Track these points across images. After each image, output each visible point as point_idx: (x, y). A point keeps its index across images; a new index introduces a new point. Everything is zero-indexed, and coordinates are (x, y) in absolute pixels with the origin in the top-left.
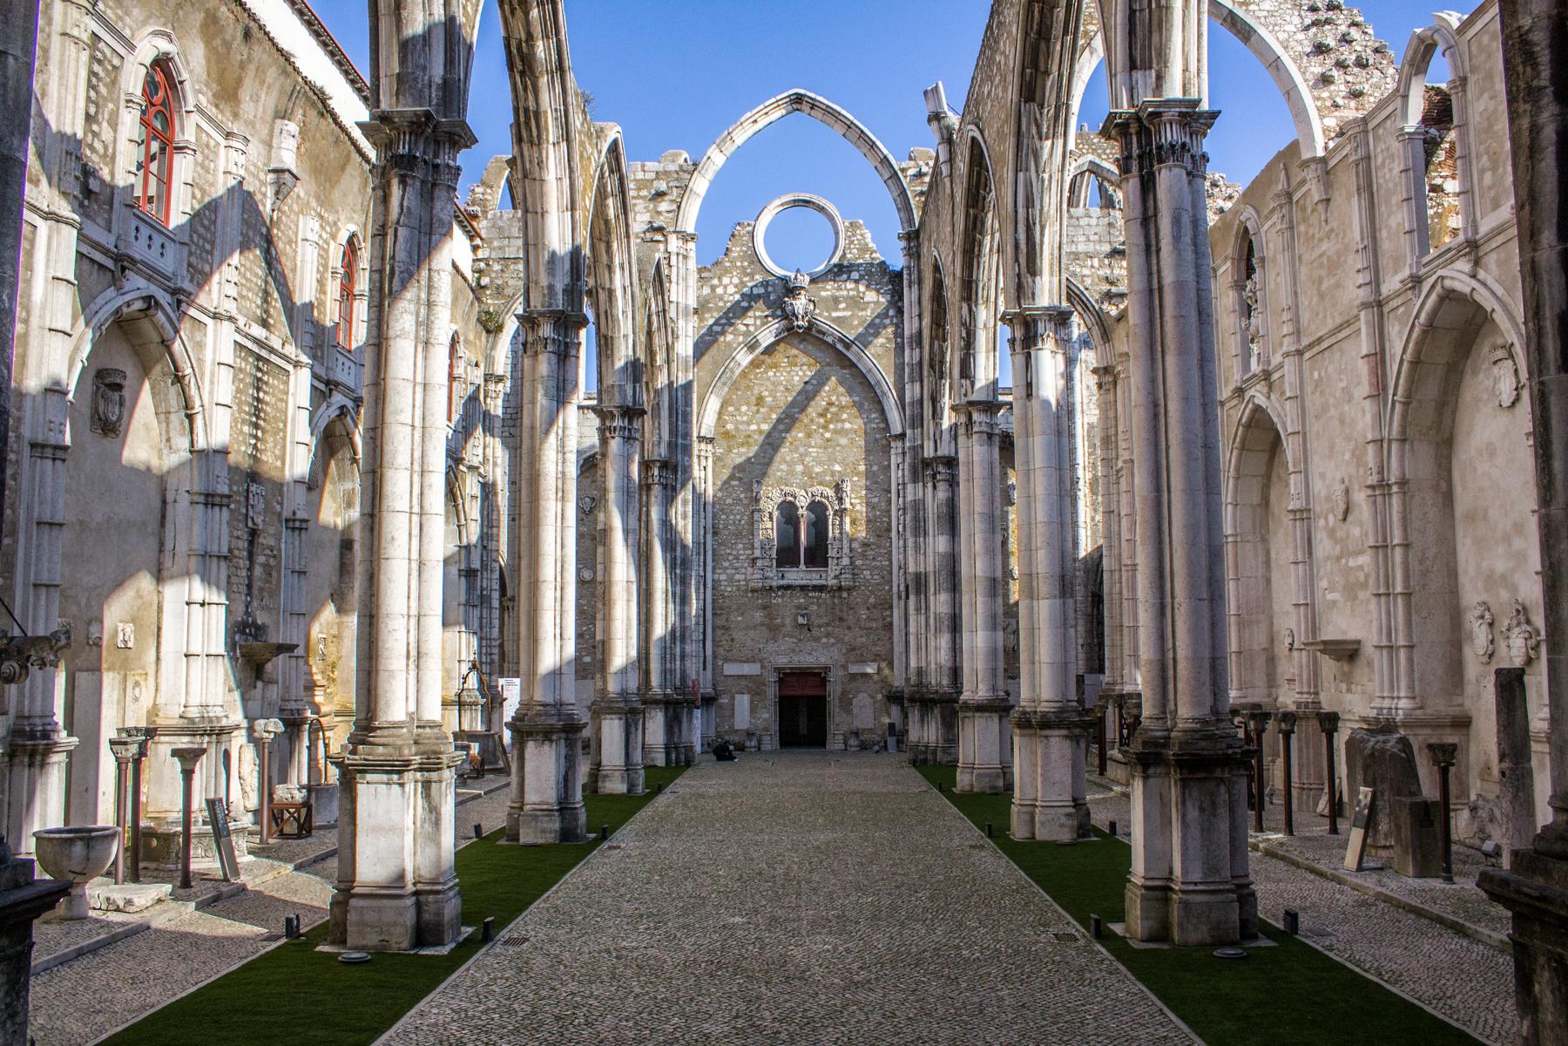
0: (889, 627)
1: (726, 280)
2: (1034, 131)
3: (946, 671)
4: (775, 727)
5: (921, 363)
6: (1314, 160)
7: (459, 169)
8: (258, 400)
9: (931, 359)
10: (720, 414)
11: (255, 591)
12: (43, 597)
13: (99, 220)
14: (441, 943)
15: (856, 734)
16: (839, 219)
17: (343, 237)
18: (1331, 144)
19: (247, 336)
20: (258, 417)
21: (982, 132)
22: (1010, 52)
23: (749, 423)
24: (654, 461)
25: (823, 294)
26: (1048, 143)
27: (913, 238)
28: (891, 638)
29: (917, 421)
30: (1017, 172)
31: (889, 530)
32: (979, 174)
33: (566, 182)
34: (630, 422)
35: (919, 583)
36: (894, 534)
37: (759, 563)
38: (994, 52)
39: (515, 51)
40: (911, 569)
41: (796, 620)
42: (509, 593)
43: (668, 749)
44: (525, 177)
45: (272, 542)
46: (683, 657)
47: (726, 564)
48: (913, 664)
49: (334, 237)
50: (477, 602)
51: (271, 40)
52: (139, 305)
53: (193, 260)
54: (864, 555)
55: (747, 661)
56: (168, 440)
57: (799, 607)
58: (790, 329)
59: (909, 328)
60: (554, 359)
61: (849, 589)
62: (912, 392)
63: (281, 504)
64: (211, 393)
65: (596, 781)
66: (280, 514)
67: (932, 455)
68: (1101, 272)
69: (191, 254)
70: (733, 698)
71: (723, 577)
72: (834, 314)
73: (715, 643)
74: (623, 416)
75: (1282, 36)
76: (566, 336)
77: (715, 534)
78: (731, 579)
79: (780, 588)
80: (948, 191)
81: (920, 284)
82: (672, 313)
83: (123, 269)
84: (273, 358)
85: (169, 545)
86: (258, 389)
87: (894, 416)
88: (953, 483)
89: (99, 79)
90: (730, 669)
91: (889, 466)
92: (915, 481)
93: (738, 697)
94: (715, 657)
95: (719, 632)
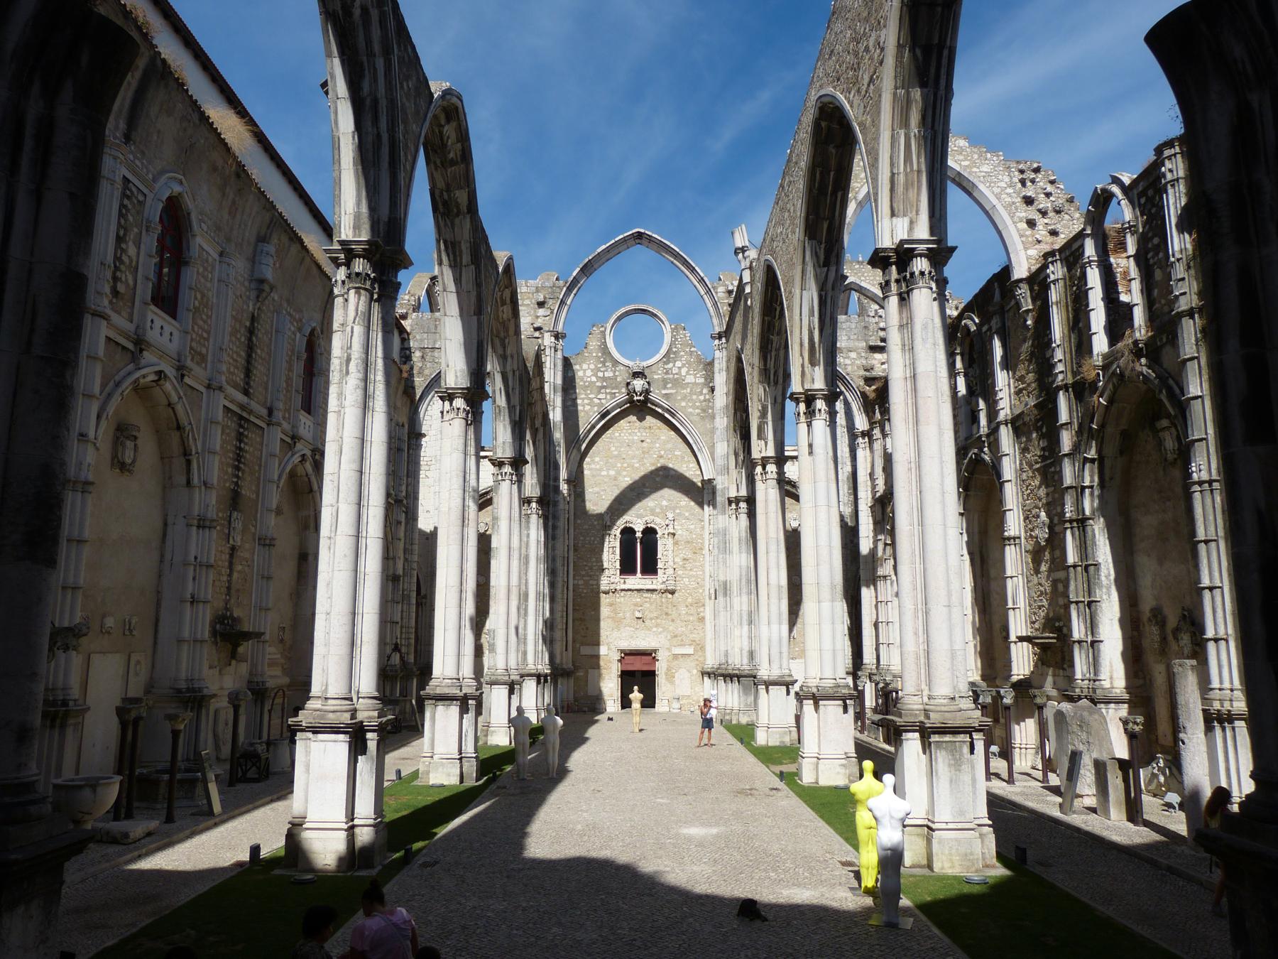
0: (702, 620)
1: (585, 366)
3: (745, 654)
6: (1021, 280)
7: (399, 284)
8: (240, 449)
11: (233, 591)
12: (69, 596)
13: (124, 314)
14: (371, 866)
16: (667, 323)
17: (307, 331)
18: (1034, 268)
19: (232, 401)
20: (239, 462)
23: (601, 470)
36: (706, 551)
40: (722, 578)
42: (423, 592)
45: (247, 555)
49: (300, 330)
50: (400, 599)
52: (152, 377)
53: (194, 344)
56: (170, 478)
57: (636, 605)
61: (673, 593)
63: (255, 527)
64: (204, 443)
66: (254, 534)
68: (858, 362)
69: (192, 340)
70: (587, 672)
71: (581, 582)
75: (997, 190)
77: (575, 550)
82: (547, 390)
83: (141, 351)
84: (252, 419)
85: (168, 556)
86: (241, 441)
88: (752, 515)
89: (128, 210)
94: (574, 641)
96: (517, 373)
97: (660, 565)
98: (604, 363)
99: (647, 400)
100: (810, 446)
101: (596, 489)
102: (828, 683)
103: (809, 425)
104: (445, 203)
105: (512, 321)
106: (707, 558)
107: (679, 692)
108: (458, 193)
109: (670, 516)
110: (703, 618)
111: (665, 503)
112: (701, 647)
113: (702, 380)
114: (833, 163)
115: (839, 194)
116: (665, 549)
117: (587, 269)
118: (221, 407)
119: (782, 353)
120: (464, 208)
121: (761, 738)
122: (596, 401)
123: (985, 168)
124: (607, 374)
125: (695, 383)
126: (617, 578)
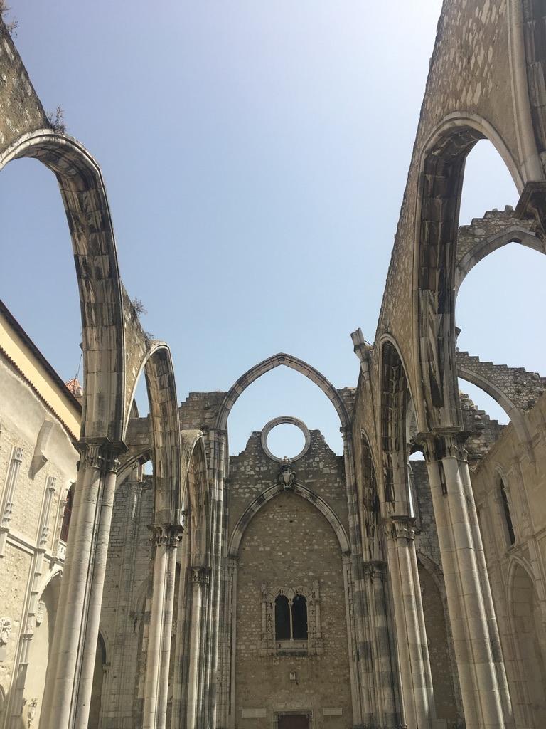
0: (348, 681)
1: (246, 463)
2: (430, 308)
5: (357, 503)
9: (364, 499)
10: (241, 541)
21: (390, 334)
22: (410, 264)
23: (259, 546)
24: (196, 568)
25: (300, 470)
26: (441, 315)
27: (347, 430)
28: (350, 689)
29: (358, 539)
30: (419, 337)
32: (388, 369)
33: (115, 353)
34: (172, 535)
35: (366, 649)
38: (395, 277)
44: (88, 350)
47: (245, 638)
48: (366, 711)
55: (258, 707)
58: (281, 491)
59: (349, 482)
61: (322, 655)
62: (352, 521)
67: (368, 559)
71: (243, 647)
72: (306, 481)
73: (237, 696)
74: (167, 531)
76: (108, 458)
77: (238, 618)
78: (247, 649)
79: (277, 655)
80: (369, 388)
87: (343, 541)
88: (384, 578)
90: (247, 713)
91: (342, 573)
94: (237, 704)
96: (175, 448)
97: (310, 629)
98: (260, 461)
100: (444, 486)
101: (255, 563)
103: (440, 466)
104: (87, 269)
105: (170, 403)
108: (99, 258)
109: (316, 584)
110: (349, 680)
111: (311, 574)
112: (348, 708)
113: (335, 471)
114: (440, 214)
115: (449, 244)
116: (313, 614)
117: (243, 382)
120: (106, 272)
122: (254, 490)
124: (262, 469)
126: (273, 644)
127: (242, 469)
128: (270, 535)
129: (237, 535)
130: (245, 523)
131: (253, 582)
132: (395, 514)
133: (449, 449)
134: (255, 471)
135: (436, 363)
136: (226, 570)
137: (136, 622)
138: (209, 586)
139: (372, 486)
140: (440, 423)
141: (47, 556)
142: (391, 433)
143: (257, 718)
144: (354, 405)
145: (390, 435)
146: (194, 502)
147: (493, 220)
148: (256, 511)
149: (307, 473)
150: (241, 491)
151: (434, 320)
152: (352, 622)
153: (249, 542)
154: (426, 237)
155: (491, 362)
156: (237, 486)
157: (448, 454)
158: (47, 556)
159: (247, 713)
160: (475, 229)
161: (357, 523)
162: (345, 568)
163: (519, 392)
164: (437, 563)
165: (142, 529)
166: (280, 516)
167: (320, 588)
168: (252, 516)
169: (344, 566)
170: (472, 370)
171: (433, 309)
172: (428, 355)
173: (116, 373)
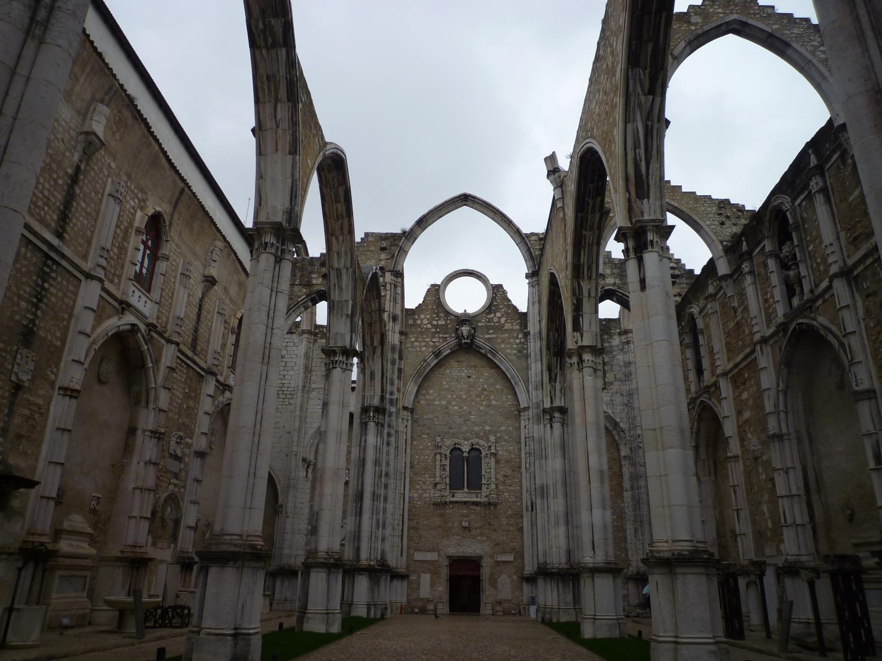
1: (422, 316)
2: (639, 89)
3: (563, 552)
4: (446, 597)
8: (43, 288)
10: (416, 394)
15: (500, 603)
17: (150, 212)
22: (620, 45)
23: (434, 400)
26: (651, 97)
28: (522, 537)
30: (626, 123)
31: (520, 467)
35: (543, 492)
36: (523, 469)
37: (439, 487)
39: (254, 31)
41: (461, 524)
42: (280, 501)
43: (369, 606)
45: (40, 401)
46: (383, 539)
47: (418, 487)
51: (92, 42)
54: (504, 483)
57: (463, 516)
60: (272, 259)
61: (495, 505)
63: (56, 375)
65: (302, 623)
66: (53, 383)
70: (419, 577)
71: (416, 495)
72: (487, 336)
73: (410, 539)
74: (343, 355)
76: (283, 245)
77: (412, 467)
78: (420, 497)
81: (540, 302)
82: (386, 316)
84: (64, 263)
86: (44, 281)
90: (418, 556)
91: (520, 427)
92: (539, 422)
93: (422, 575)
94: (409, 548)
95: (412, 531)
96: (350, 270)
97: (484, 481)
98: (437, 314)
99: (472, 342)
101: (431, 416)
102: (685, 547)
103: (640, 260)
106: (524, 474)
107: (500, 597)
109: (492, 438)
110: (521, 530)
111: (487, 428)
112: (520, 555)
113: (518, 327)
115: (664, 15)
116: (488, 467)
117: (423, 223)
118: (19, 236)
119: (595, 248)
121: (588, 631)
122: (431, 343)
123: (796, 31)
124: (440, 323)
125: (512, 330)
127: (419, 322)
128: (446, 389)
129: (412, 388)
130: (420, 376)
131: (428, 434)
132: (586, 343)
133: (652, 242)
134: (432, 325)
135: (642, 151)
136: (400, 420)
137: (308, 467)
138: (383, 425)
139: (557, 331)
140: (643, 216)
141: (217, 381)
142: (584, 259)
143: (428, 561)
144: (542, 250)
145: (582, 261)
146: (368, 342)
147: (712, 7)
148: (432, 365)
149: (488, 328)
150: (416, 344)
151: (643, 102)
152: (528, 475)
153: (424, 395)
154: (640, 5)
155: (694, 193)
156: (413, 340)
157: (650, 249)
158: (217, 381)
159: (418, 556)
160: (691, 16)
161: (540, 370)
162: (523, 423)
163: (722, 224)
164: (618, 420)
165: (313, 378)
166: (460, 373)
167: (496, 442)
168: (428, 370)
169: (522, 422)
170: (673, 200)
171: (642, 90)
172: (635, 142)
173: (289, 158)
